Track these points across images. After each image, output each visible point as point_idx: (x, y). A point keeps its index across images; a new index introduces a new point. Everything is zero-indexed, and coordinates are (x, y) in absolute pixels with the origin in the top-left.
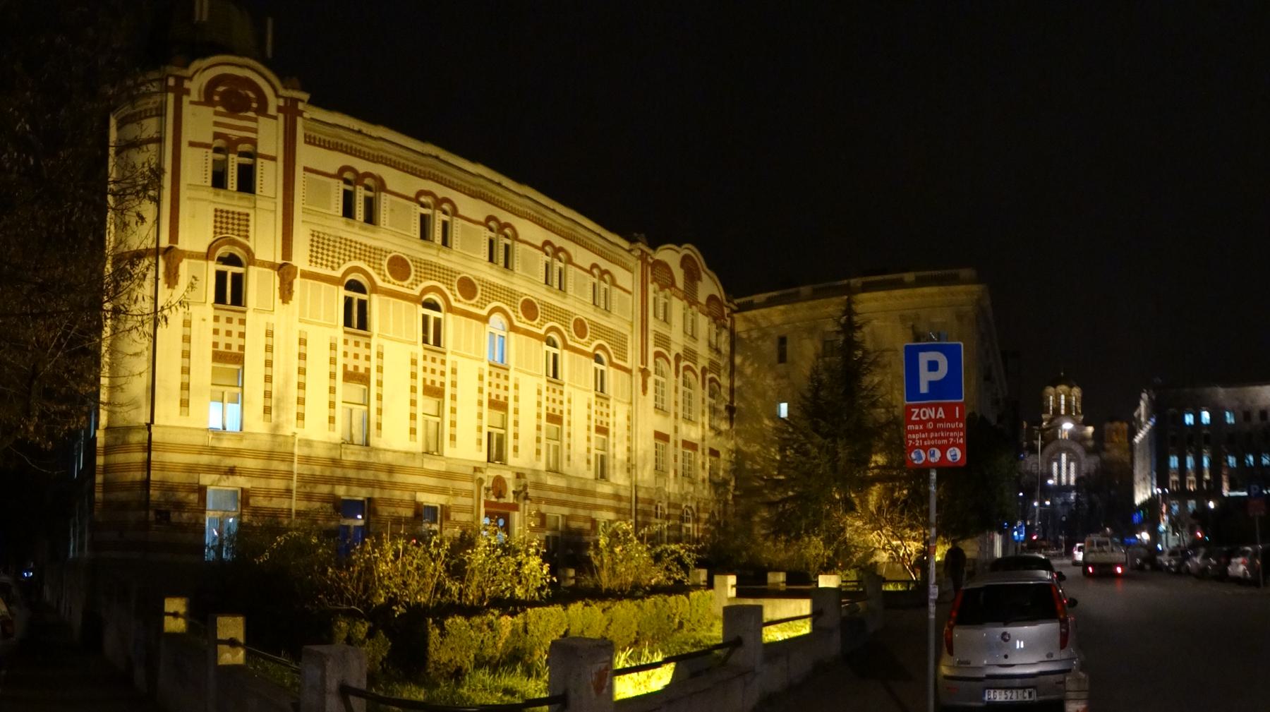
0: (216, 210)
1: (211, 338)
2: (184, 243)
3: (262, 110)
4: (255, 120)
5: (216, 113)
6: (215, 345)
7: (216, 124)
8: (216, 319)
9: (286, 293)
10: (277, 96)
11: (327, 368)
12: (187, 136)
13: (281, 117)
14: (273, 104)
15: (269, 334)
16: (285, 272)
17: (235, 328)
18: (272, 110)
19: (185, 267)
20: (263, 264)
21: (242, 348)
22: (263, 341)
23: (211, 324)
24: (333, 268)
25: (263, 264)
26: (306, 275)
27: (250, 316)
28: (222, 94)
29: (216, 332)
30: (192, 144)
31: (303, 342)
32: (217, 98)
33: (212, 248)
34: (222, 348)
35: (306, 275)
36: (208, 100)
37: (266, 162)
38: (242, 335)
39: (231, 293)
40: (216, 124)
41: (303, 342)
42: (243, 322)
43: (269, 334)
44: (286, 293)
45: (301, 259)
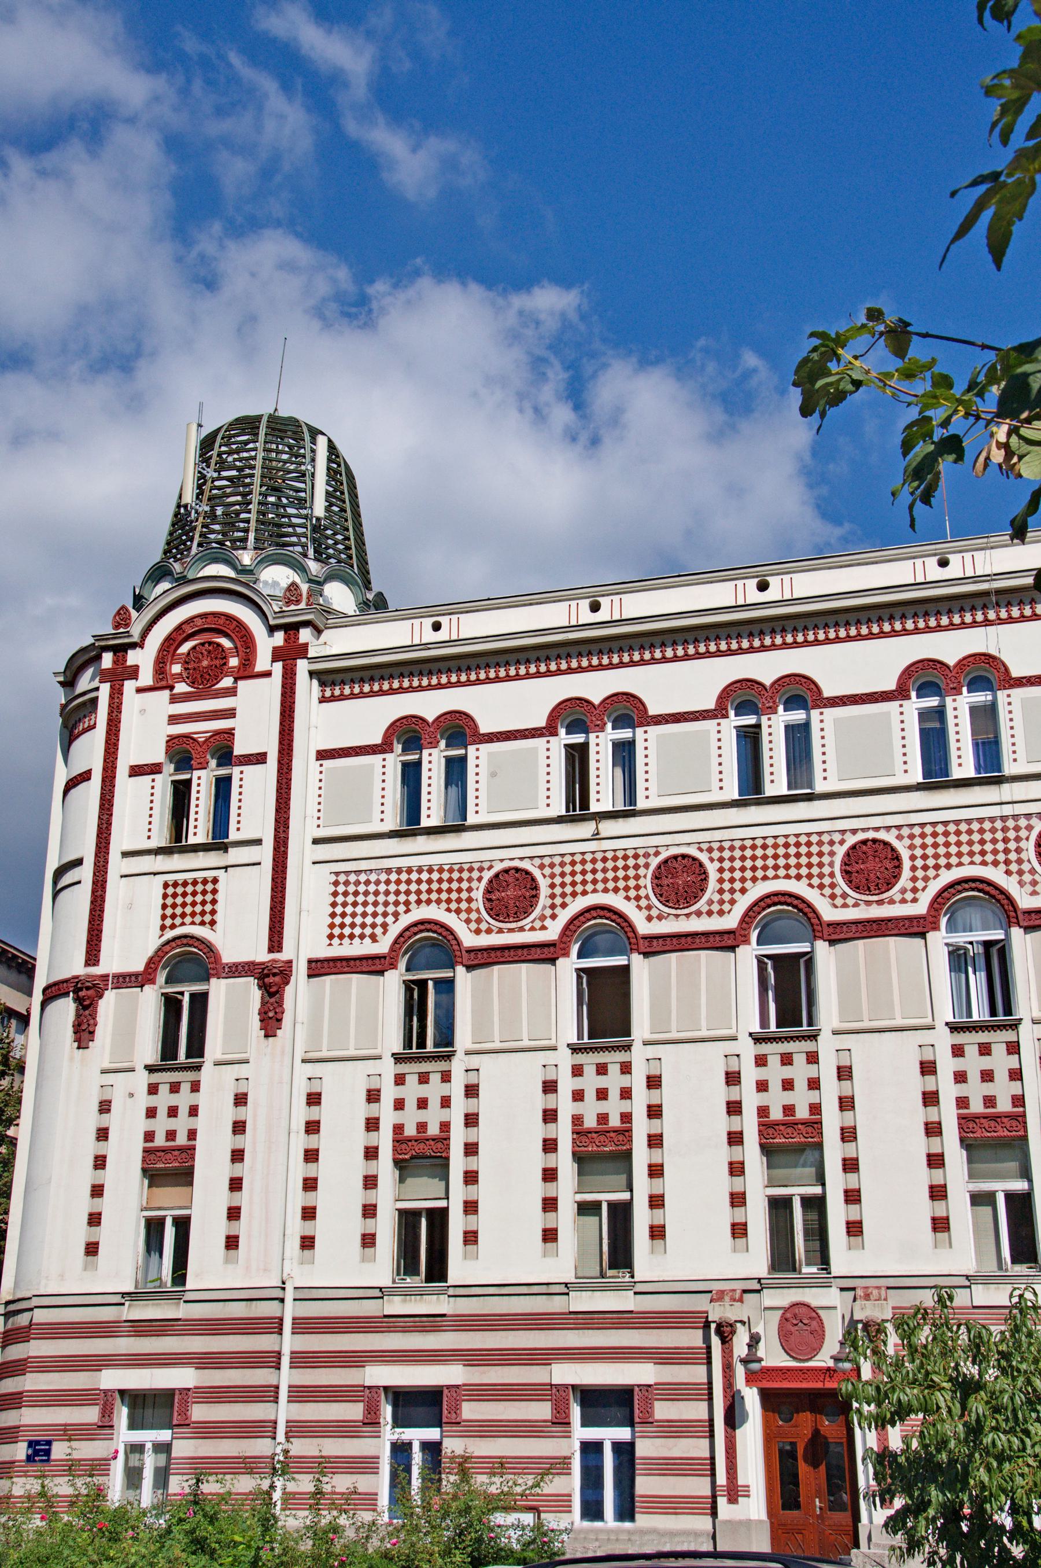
0: (166, 885)
1: (143, 1124)
2: (111, 963)
3: (247, 672)
4: (232, 692)
5: (174, 699)
6: (149, 1136)
7: (173, 719)
8: (153, 1089)
9: (271, 1020)
10: (272, 629)
11: (361, 1139)
12: (125, 761)
13: (278, 668)
14: (266, 644)
15: (241, 1100)
16: (272, 980)
17: (183, 1100)
18: (263, 661)
19: (109, 1004)
20: (238, 970)
21: (192, 1134)
22: (229, 1113)
23: (144, 1101)
24: (373, 938)
25: (238, 970)
26: (318, 968)
27: (207, 1074)
28: (186, 661)
29: (151, 1113)
30: (136, 771)
31: (314, 1099)
32: (177, 669)
33: (152, 964)
34: (160, 1141)
35: (318, 968)
36: (162, 681)
37: (251, 771)
38: (194, 1111)
39: (183, 1037)
40: (173, 719)
41: (314, 1099)
42: (195, 1087)
43: (241, 1100)
44: (271, 1020)
45: (308, 937)
